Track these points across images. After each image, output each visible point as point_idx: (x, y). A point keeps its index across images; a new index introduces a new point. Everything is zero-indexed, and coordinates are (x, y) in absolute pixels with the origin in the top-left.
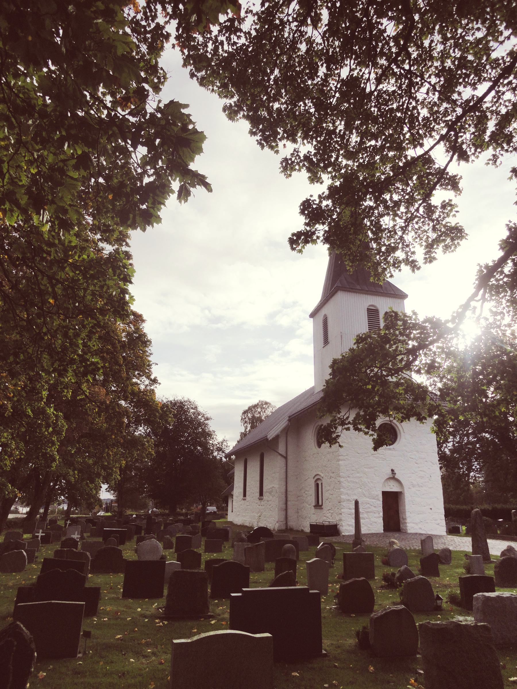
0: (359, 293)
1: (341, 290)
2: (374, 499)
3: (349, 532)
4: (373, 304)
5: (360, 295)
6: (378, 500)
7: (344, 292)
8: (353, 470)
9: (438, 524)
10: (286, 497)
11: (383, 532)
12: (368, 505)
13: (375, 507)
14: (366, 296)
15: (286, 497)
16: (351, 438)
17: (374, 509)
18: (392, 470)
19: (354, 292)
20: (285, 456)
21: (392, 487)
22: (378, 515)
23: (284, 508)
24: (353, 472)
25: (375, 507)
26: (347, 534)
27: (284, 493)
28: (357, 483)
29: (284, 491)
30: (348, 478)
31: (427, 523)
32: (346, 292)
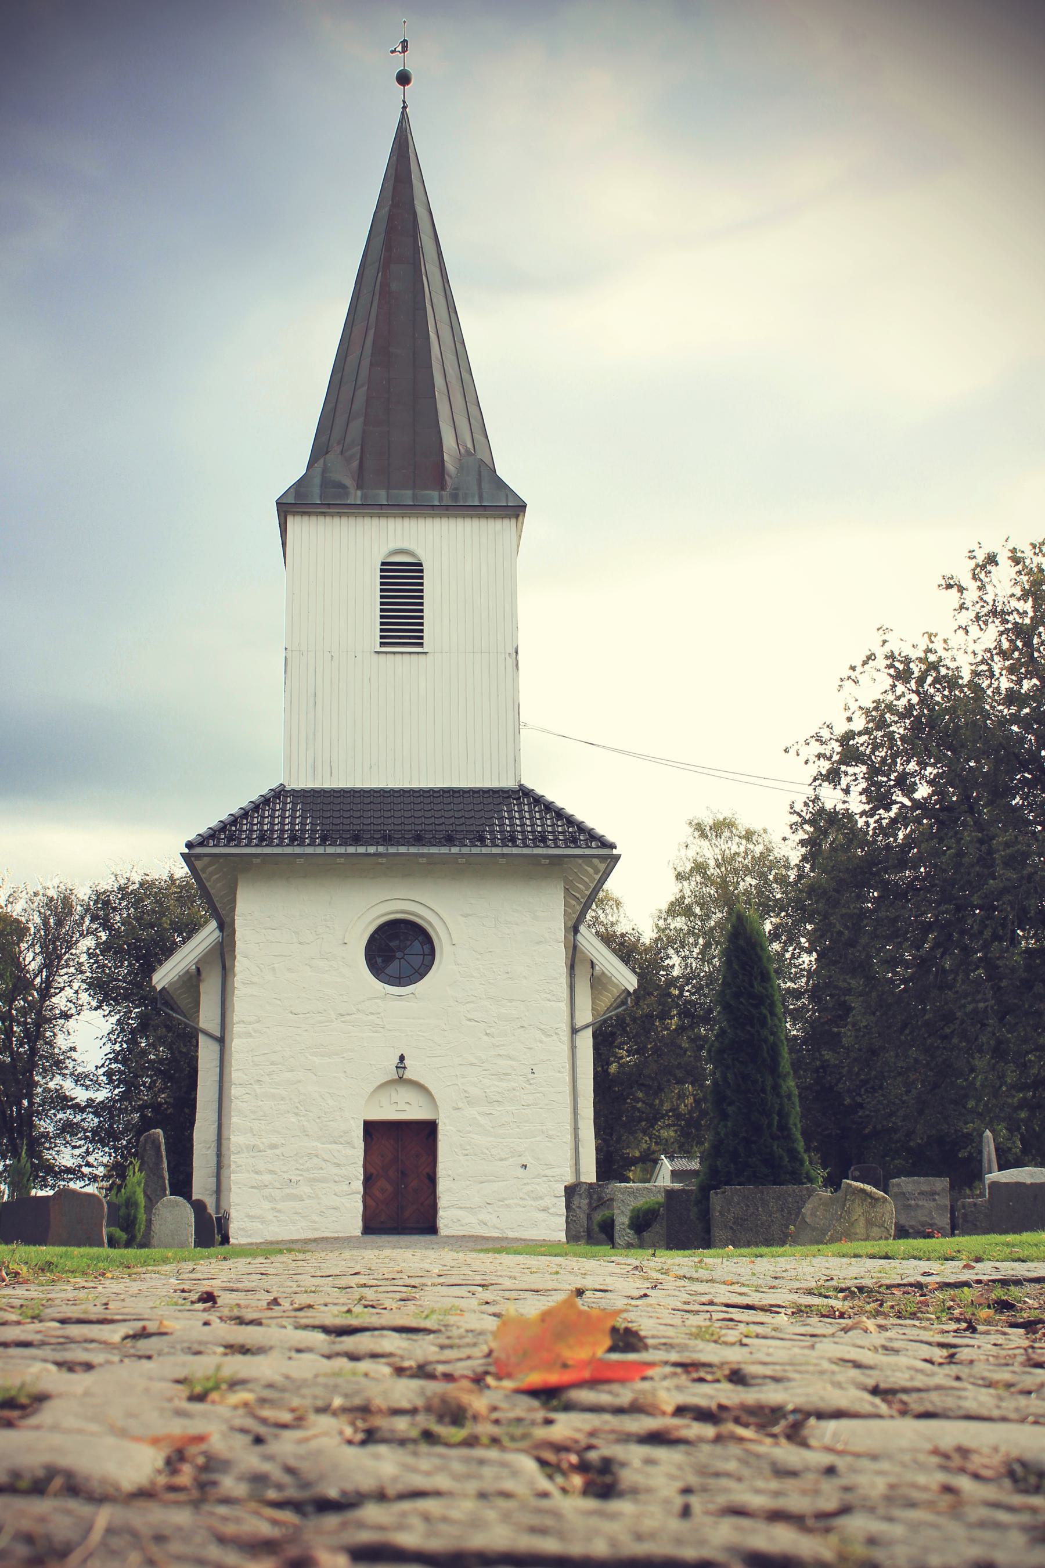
0: (355, 515)
1: (295, 514)
2: (336, 1143)
3: (249, 1237)
4: (405, 545)
5: (360, 520)
6: (350, 1144)
7: (306, 518)
8: (272, 1063)
9: (545, 1210)
10: (219, 1155)
11: (360, 1234)
12: (315, 1160)
13: (338, 1165)
14: (383, 521)
15: (219, 1155)
16: (273, 969)
17: (334, 1170)
18: (402, 1058)
19: (340, 515)
20: (218, 1035)
21: (402, 1106)
22: (345, 1187)
23: (215, 1188)
24: (273, 1068)
25: (338, 1165)
26: (243, 1241)
27: (214, 1145)
28: (283, 1099)
29: (214, 1137)
30: (256, 1087)
31: (508, 1206)
32: (313, 519)
